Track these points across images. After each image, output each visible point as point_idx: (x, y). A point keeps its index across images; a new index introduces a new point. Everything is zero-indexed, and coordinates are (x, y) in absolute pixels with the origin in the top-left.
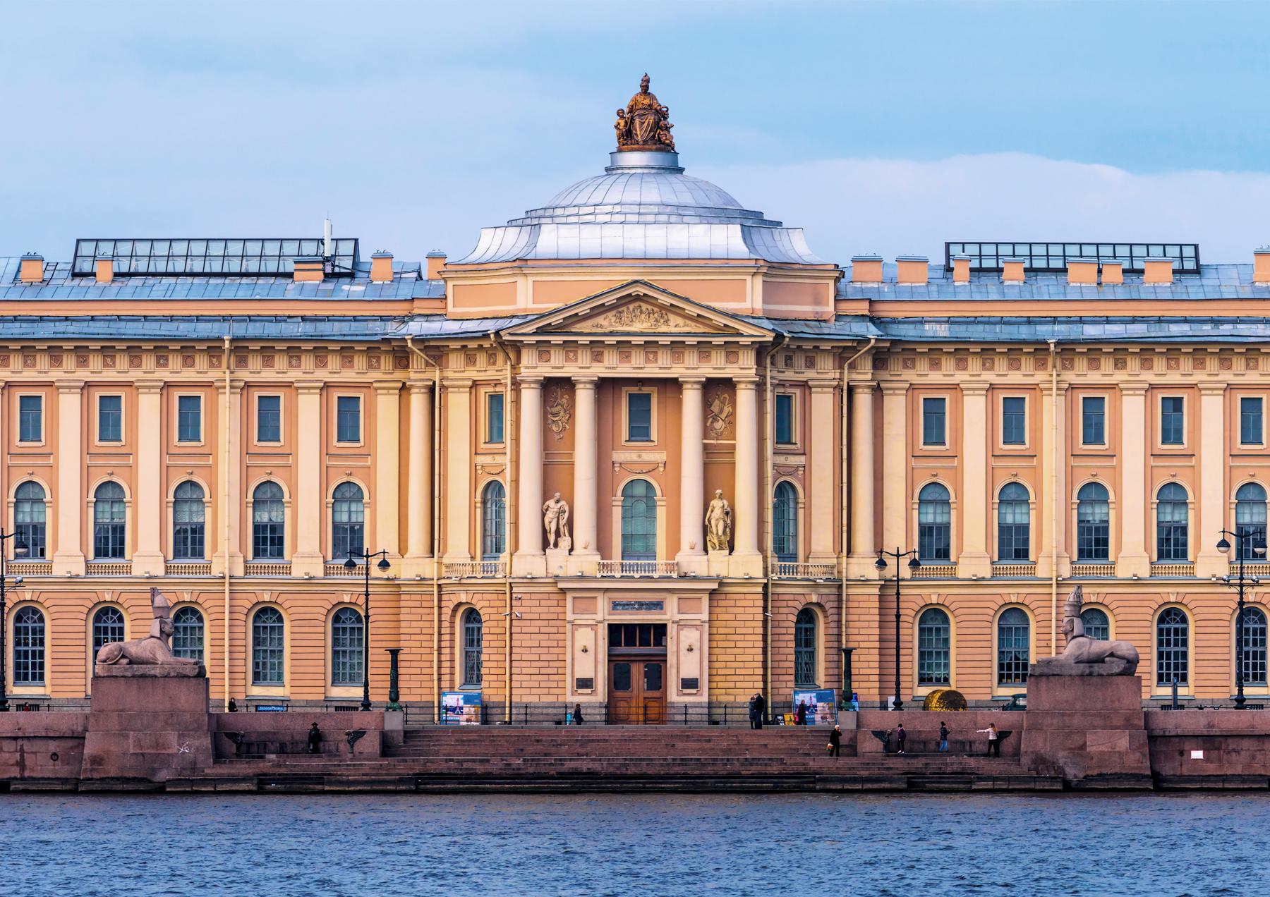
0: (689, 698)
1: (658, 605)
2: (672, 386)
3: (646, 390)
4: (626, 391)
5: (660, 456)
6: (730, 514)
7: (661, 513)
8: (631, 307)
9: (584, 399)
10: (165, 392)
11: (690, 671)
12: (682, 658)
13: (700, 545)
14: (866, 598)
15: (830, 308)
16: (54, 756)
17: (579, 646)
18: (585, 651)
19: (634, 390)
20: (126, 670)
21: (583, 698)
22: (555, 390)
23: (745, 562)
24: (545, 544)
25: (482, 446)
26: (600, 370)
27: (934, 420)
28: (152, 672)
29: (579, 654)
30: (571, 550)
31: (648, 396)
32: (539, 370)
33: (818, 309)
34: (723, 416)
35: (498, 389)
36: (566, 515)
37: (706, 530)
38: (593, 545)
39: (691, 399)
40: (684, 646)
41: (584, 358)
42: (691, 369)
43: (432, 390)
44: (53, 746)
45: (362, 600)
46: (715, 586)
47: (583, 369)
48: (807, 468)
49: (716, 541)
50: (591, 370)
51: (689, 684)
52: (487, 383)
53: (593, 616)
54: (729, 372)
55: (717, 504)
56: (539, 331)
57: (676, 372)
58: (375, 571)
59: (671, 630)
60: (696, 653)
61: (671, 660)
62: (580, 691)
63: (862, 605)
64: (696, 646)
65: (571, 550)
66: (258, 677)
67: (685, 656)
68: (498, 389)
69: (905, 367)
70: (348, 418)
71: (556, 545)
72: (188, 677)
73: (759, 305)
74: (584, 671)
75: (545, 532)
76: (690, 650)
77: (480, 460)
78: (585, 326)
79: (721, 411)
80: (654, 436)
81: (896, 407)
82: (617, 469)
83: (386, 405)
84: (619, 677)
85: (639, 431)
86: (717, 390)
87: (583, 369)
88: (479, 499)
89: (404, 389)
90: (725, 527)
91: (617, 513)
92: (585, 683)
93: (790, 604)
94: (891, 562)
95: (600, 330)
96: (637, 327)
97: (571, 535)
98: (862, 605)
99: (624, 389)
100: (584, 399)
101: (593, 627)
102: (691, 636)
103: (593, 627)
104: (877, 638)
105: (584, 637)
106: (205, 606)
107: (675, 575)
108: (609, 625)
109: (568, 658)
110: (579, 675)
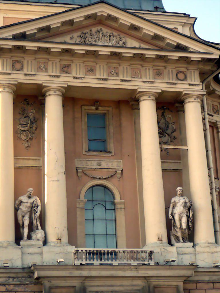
6: (190, 208)
8: (94, 30)
9: (53, 106)
13: (165, 239)
24: (18, 238)
26: (67, 80)
32: (13, 76)
36: (39, 208)
37: (170, 224)
39: (148, 111)
41: (54, 69)
42: (150, 85)
47: (54, 80)
49: (179, 234)
50: (61, 79)
54: (182, 87)
55: (179, 202)
56: (15, 38)
57: (137, 85)
65: (45, 243)
71: (29, 237)
75: (18, 227)
80: (111, 146)
86: (170, 107)
90: (188, 221)
97: (43, 228)
100: (53, 106)
107: (152, 263)
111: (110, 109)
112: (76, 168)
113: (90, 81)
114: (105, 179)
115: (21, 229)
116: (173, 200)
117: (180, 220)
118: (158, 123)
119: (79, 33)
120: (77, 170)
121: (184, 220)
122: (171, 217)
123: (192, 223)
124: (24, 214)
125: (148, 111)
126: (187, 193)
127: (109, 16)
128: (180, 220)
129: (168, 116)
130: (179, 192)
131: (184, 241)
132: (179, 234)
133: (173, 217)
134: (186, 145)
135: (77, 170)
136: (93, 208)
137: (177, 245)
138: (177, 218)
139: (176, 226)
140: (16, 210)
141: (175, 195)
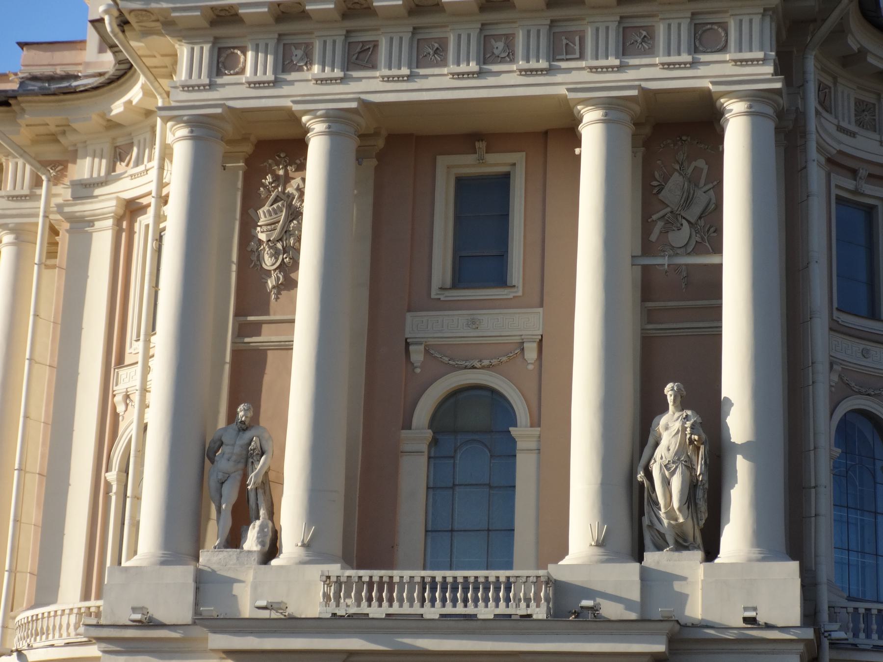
3: (496, 162)
5: (527, 323)
19: (467, 164)
31: (503, 181)
54: (708, 73)
55: (671, 428)
71: (234, 540)
79: (688, 202)
82: (417, 355)
91: (414, 475)
99: (442, 161)
111: (519, 158)
112: (406, 339)
113: (442, 84)
114: (488, 367)
120: (407, 344)
121: (676, 483)
124: (220, 476)
128: (667, 483)
129: (694, 164)
133: (649, 475)
135: (407, 344)
136: (455, 451)
139: (657, 503)
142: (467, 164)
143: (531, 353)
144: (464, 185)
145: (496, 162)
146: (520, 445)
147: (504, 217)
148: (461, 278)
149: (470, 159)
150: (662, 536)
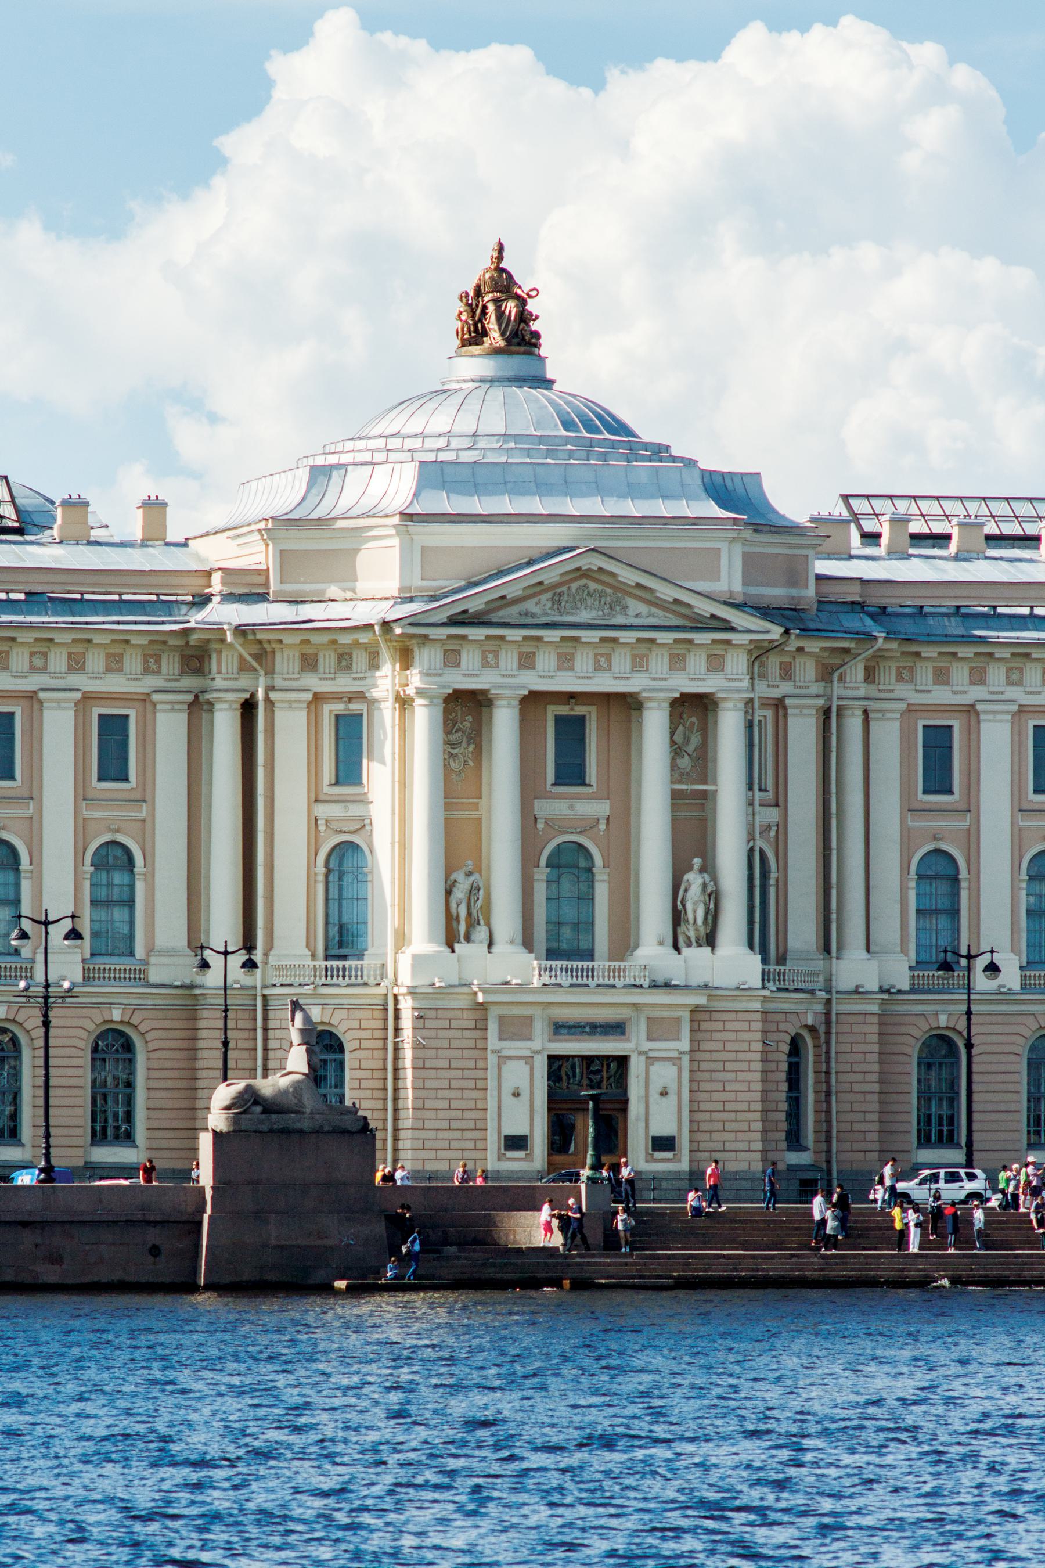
0: (663, 1164)
1: (617, 1028)
2: (626, 706)
3: (579, 710)
4: (554, 710)
5: (601, 808)
7: (602, 892)
9: (504, 723)
10: (313, 707)
11: (664, 1124)
12: (653, 1108)
14: (860, 1019)
15: (811, 592)
16: (155, 1251)
17: (507, 1088)
18: (516, 1094)
19: (564, 710)
20: (261, 1122)
21: (515, 1163)
22: (464, 712)
23: (733, 963)
25: (326, 789)
27: (938, 759)
28: (298, 1126)
29: (507, 1100)
30: (490, 945)
31: (581, 720)
33: (794, 592)
34: (690, 748)
35: (354, 707)
37: (677, 917)
38: (519, 939)
39: (655, 727)
40: (655, 1088)
43: (248, 708)
44: (152, 1236)
45: (962, 1026)
46: (702, 1000)
47: (505, 679)
48: (782, 827)
49: (692, 934)
51: (663, 1144)
52: (336, 697)
53: (528, 1044)
55: (694, 880)
58: (981, 982)
59: (636, 1068)
60: (672, 1098)
61: (635, 1108)
62: (510, 1154)
63: (855, 1028)
64: (673, 1088)
66: (100, 1136)
67: (654, 1105)
68: (354, 707)
69: (900, 679)
70: (112, 747)
72: (349, 1132)
73: (738, 587)
74: (515, 1127)
75: (450, 919)
76: (664, 1093)
77: (323, 811)
78: (510, 614)
79: (687, 740)
81: (888, 736)
82: (541, 825)
83: (170, 728)
84: (561, 1135)
85: (571, 772)
87: (505, 679)
88: (321, 869)
89: (199, 707)
90: (706, 914)
92: (516, 1143)
93: (782, 1027)
94: (216, 961)
95: (529, 620)
96: (584, 616)
98: (855, 1028)
100: (504, 723)
101: (529, 1060)
102: (664, 1075)
103: (529, 1060)
104: (875, 1077)
105: (516, 1075)
106: (143, 1028)
108: (550, 1057)
109: (491, 1105)
110: (509, 1130)
111: (593, 709)
114: (581, 832)
115: (454, 923)
116: (686, 877)
117: (695, 912)
118: (672, 733)
119: (549, 595)
122: (680, 907)
123: (713, 916)
125: (655, 727)
126: (709, 868)
127: (600, 569)
128: (695, 912)
130: (696, 867)
131: (699, 945)
132: (692, 934)
133: (684, 906)
134: (715, 783)
137: (685, 951)
138: (689, 906)
140: (448, 892)
141: (690, 868)
142: (564, 710)
143: (602, 826)
144: (559, 720)
145: (579, 710)
146: (597, 877)
147: (582, 740)
148: (560, 780)
149: (567, 707)
150: (689, 938)
